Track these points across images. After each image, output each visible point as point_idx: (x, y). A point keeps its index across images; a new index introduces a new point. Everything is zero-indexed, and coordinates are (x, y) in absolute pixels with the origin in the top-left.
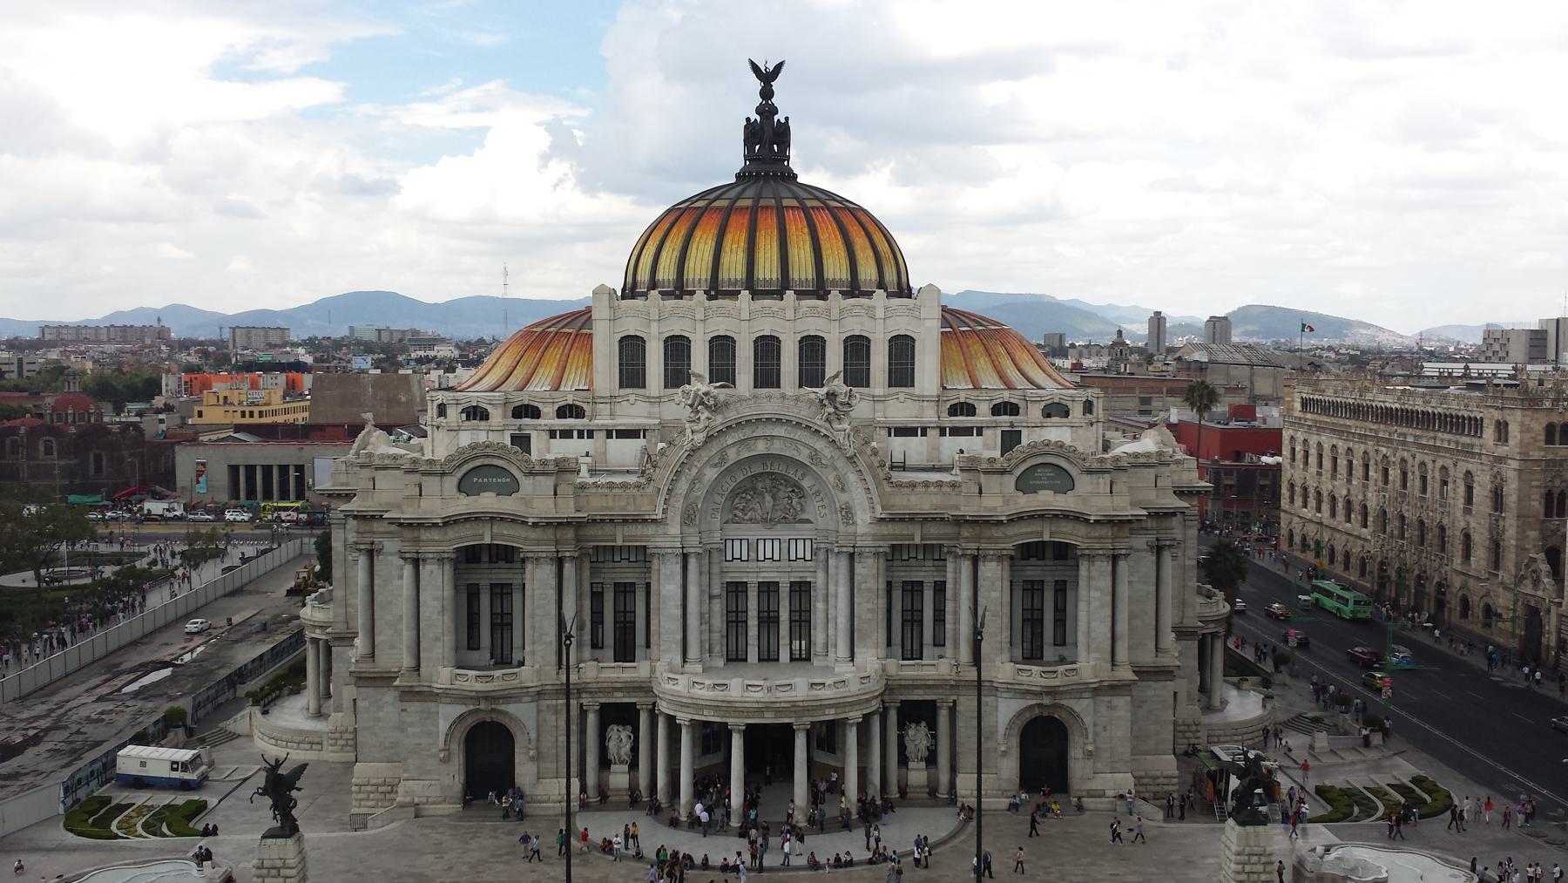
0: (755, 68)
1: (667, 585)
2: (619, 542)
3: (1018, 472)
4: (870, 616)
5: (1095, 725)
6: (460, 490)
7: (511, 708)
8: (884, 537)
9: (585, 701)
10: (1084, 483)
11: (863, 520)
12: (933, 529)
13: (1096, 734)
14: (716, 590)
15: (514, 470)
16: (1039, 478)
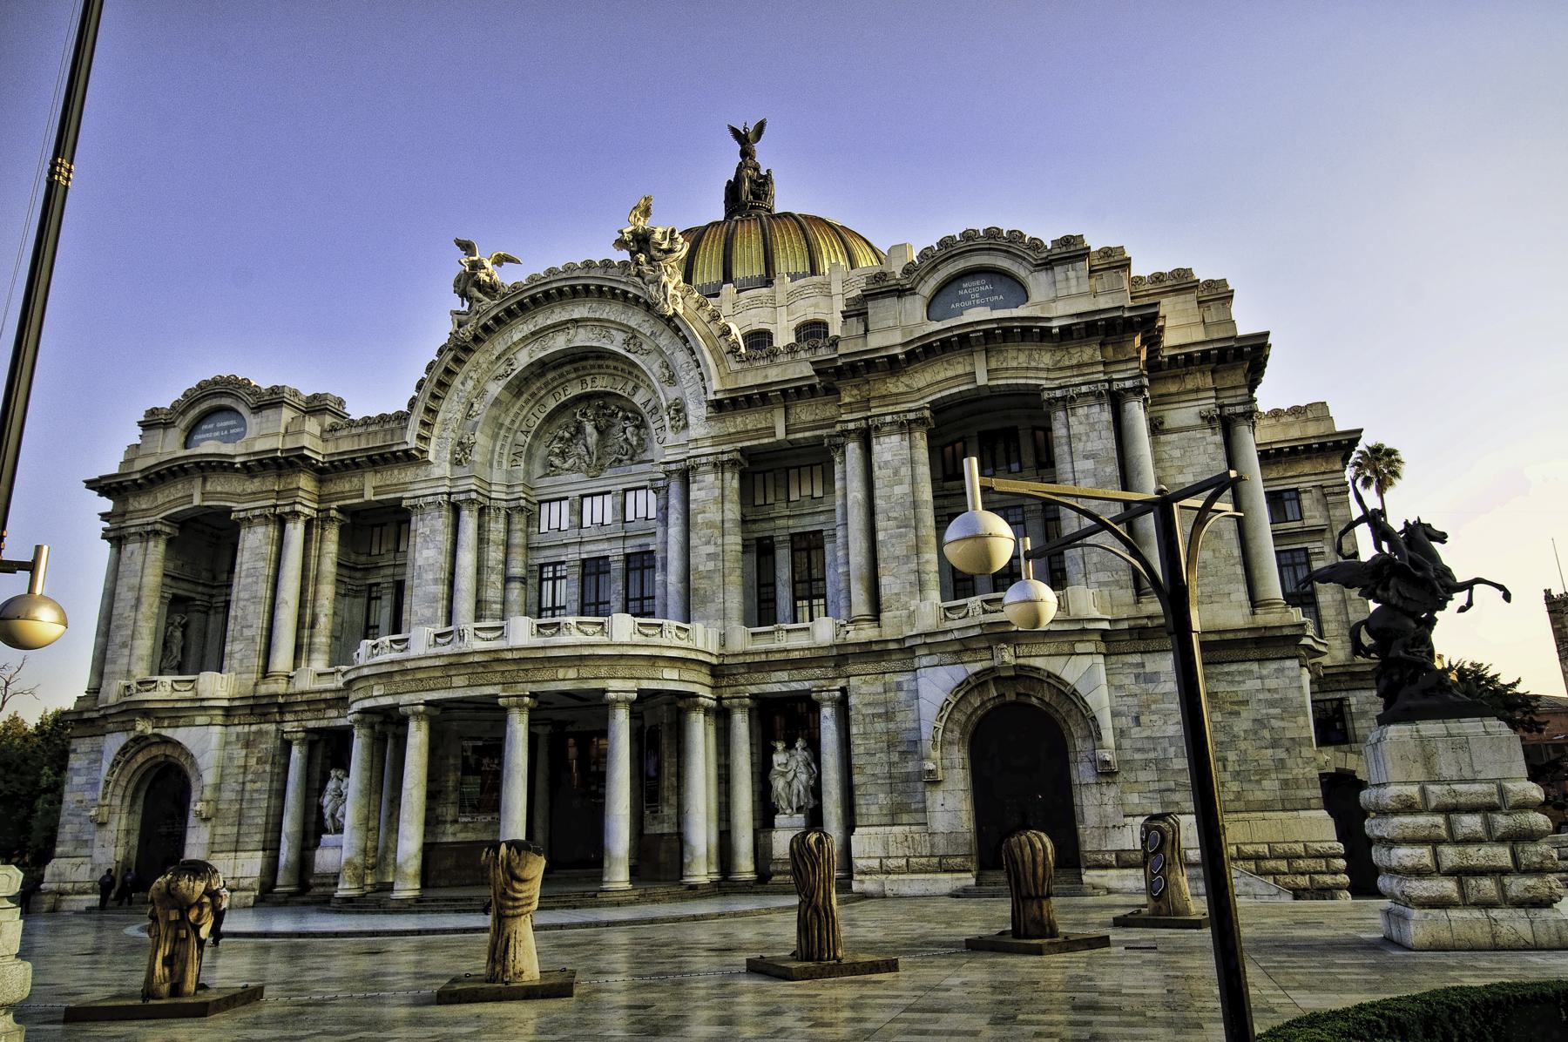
0: (735, 133)
1: (426, 549)
2: (369, 495)
3: (928, 288)
4: (711, 565)
5: (1115, 714)
6: (186, 446)
7: (179, 734)
8: (730, 437)
9: (288, 727)
10: (1039, 285)
11: (697, 412)
12: (805, 413)
13: (1121, 733)
14: (517, 569)
15: (242, 409)
16: (968, 298)
